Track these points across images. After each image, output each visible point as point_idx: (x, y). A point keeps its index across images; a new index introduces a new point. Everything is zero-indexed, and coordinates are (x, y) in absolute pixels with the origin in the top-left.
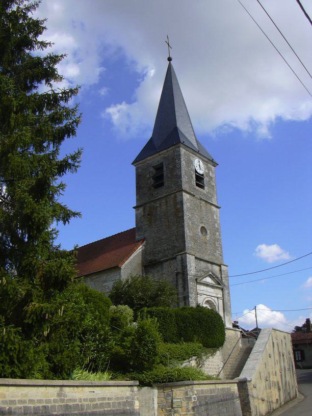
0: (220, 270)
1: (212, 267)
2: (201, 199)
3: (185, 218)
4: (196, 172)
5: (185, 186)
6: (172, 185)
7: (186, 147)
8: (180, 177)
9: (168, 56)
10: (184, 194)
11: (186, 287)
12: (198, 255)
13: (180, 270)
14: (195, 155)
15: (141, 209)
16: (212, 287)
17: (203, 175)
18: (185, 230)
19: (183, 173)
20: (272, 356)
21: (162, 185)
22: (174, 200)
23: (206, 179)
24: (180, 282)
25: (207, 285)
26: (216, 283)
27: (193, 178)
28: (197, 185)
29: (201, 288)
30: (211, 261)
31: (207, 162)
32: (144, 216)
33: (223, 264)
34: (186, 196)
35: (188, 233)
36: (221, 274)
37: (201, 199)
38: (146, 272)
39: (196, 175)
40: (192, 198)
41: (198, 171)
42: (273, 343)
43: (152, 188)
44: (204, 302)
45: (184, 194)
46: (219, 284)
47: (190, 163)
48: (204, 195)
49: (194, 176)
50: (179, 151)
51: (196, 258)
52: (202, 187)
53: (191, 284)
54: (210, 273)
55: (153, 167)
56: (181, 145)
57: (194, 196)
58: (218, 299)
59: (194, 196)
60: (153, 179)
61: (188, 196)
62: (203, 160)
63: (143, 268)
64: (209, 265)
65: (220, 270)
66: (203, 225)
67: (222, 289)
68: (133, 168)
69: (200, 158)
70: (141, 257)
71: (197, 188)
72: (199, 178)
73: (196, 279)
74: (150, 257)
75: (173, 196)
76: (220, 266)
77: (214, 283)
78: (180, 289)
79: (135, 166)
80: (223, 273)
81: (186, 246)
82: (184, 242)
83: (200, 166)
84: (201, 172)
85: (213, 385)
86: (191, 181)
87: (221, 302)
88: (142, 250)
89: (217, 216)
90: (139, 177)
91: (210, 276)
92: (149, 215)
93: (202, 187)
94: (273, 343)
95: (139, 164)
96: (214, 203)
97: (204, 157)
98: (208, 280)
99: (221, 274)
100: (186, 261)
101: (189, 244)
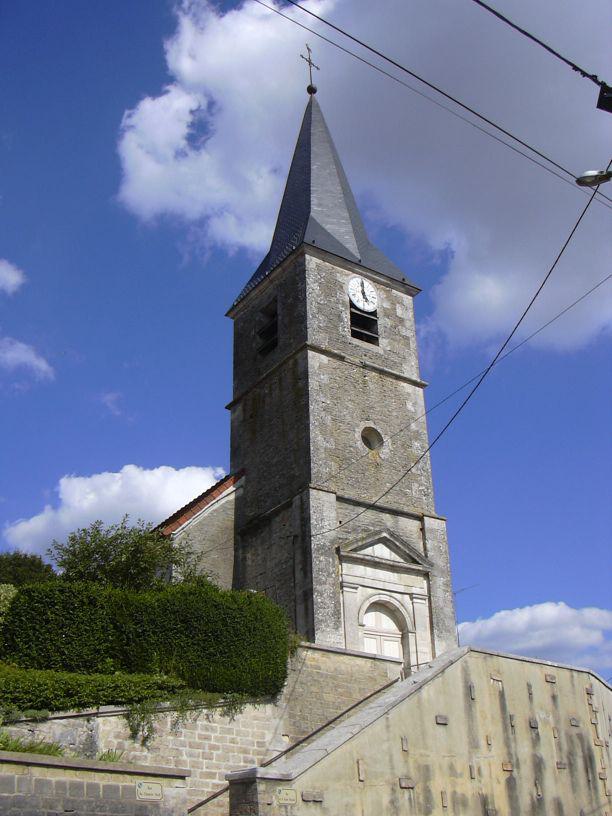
0: (422, 529)
1: (397, 522)
2: (365, 366)
3: (311, 407)
4: (352, 305)
5: (315, 336)
6: (292, 341)
7: (322, 253)
8: (303, 318)
9: (309, 84)
10: (311, 353)
11: (308, 568)
12: (350, 494)
13: (298, 531)
14: (349, 270)
15: (240, 408)
16: (393, 568)
17: (374, 313)
18: (312, 435)
19: (311, 308)
20: (430, 722)
21: (275, 344)
22: (294, 372)
23: (383, 323)
24: (299, 558)
25: (376, 564)
26: (405, 559)
27: (342, 320)
28: (355, 334)
29: (352, 572)
30: (394, 507)
31: (387, 285)
32: (244, 420)
33: (426, 513)
34: (315, 360)
35: (318, 439)
36: (424, 539)
37: (365, 366)
38: (244, 547)
39: (352, 313)
40: (337, 363)
41: (360, 304)
42: (469, 689)
43: (259, 357)
44: (367, 604)
45: (311, 353)
46: (415, 562)
47: (333, 287)
48: (377, 356)
49: (346, 317)
50: (302, 265)
51: (340, 499)
52: (374, 340)
53: (319, 561)
54: (384, 534)
55: (261, 311)
56: (306, 249)
57: (342, 358)
58: (412, 599)
59: (342, 358)
60: (260, 336)
61: (324, 359)
62: (374, 281)
63: (239, 538)
64: (387, 518)
65: (422, 529)
66: (371, 424)
67: (426, 575)
68: (230, 323)
69: (366, 277)
70: (232, 513)
71: (356, 341)
72: (364, 325)
73: (338, 550)
74: (251, 511)
75: (291, 362)
76: (420, 518)
77: (398, 558)
78: (299, 575)
79: (233, 318)
80: (428, 535)
81: (313, 471)
82: (308, 462)
83: (363, 293)
84: (369, 308)
85: (20, 768)
86: (336, 327)
87: (422, 607)
88: (237, 499)
89: (414, 404)
90: (239, 337)
91: (384, 541)
92: (251, 417)
93: (374, 340)
94: (469, 689)
95: (237, 313)
96: (406, 375)
97: (377, 273)
98: (381, 551)
99: (424, 539)
100: (308, 507)
101: (321, 464)
